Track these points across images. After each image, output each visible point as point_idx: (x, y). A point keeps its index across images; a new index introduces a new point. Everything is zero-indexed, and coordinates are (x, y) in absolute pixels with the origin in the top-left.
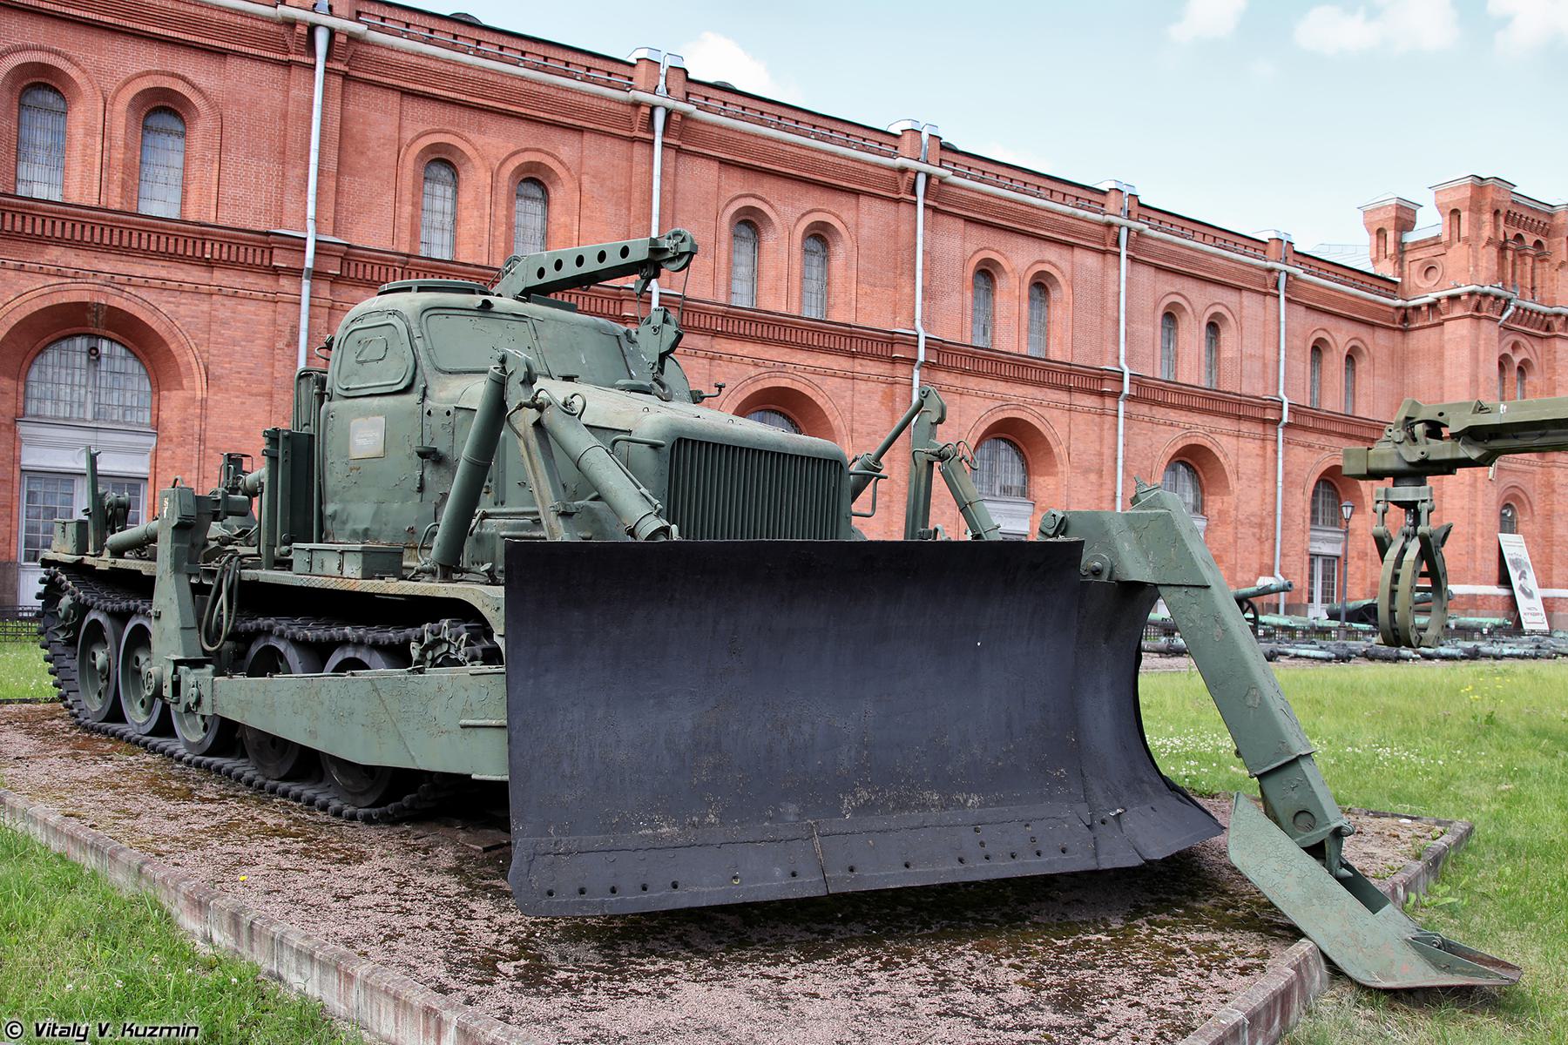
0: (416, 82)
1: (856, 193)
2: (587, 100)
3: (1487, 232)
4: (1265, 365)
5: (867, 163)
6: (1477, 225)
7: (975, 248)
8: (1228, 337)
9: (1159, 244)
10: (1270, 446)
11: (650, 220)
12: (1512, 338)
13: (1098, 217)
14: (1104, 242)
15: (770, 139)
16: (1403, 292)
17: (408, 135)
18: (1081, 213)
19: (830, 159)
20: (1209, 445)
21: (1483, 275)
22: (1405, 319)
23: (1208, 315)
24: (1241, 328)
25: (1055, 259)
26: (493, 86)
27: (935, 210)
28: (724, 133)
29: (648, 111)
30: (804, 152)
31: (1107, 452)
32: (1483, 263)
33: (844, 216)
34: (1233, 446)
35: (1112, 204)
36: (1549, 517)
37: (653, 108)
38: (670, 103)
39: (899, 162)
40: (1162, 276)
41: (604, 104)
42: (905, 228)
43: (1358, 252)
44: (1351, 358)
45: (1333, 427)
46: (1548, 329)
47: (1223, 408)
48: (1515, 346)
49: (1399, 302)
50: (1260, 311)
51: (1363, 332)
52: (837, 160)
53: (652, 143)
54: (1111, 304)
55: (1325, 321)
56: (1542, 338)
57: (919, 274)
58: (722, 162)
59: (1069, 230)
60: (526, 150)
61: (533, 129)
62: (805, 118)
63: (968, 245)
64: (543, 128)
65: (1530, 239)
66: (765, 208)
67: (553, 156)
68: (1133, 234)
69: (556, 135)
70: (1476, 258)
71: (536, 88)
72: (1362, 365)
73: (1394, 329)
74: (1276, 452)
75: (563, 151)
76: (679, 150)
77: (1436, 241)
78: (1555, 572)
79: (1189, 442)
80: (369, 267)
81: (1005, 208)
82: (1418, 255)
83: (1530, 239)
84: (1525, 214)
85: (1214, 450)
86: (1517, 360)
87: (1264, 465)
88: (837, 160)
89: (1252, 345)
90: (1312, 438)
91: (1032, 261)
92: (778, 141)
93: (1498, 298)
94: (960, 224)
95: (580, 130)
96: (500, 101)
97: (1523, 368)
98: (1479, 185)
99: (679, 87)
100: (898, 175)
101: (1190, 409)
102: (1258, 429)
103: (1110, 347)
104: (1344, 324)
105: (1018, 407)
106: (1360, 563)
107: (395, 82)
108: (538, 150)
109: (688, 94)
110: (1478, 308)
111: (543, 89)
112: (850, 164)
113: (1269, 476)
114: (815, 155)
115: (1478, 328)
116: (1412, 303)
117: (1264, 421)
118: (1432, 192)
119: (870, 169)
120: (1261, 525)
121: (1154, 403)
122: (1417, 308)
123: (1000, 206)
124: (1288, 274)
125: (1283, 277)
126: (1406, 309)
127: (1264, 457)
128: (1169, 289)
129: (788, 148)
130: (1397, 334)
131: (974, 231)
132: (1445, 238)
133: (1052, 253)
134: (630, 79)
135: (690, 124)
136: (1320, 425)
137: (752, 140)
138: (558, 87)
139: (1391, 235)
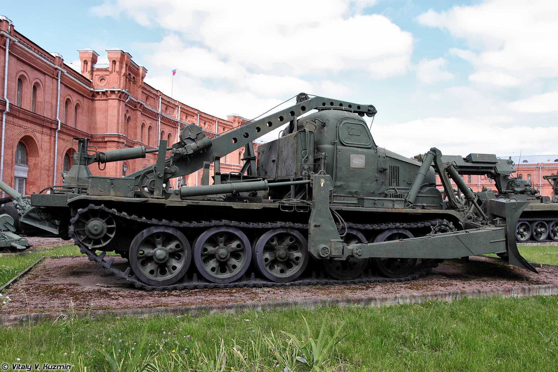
4: (52, 106)
6: (121, 68)
8: (39, 92)
20: (33, 136)
21: (122, 86)
22: (93, 96)
23: (34, 83)
24: (44, 90)
34: (42, 139)
43: (77, 66)
46: (135, 107)
47: (38, 122)
49: (92, 89)
55: (70, 92)
56: (133, 110)
65: (132, 76)
70: (120, 80)
72: (79, 111)
74: (55, 141)
77: (106, 70)
82: (99, 73)
85: (34, 138)
87: (50, 146)
89: (48, 98)
93: (126, 94)
98: (123, 54)
101: (27, 121)
102: (48, 131)
110: (120, 97)
113: (52, 150)
115: (120, 104)
116: (96, 90)
120: (49, 170)
122: (98, 93)
126: (94, 92)
127: (50, 143)
130: (90, 101)
139: (89, 64)
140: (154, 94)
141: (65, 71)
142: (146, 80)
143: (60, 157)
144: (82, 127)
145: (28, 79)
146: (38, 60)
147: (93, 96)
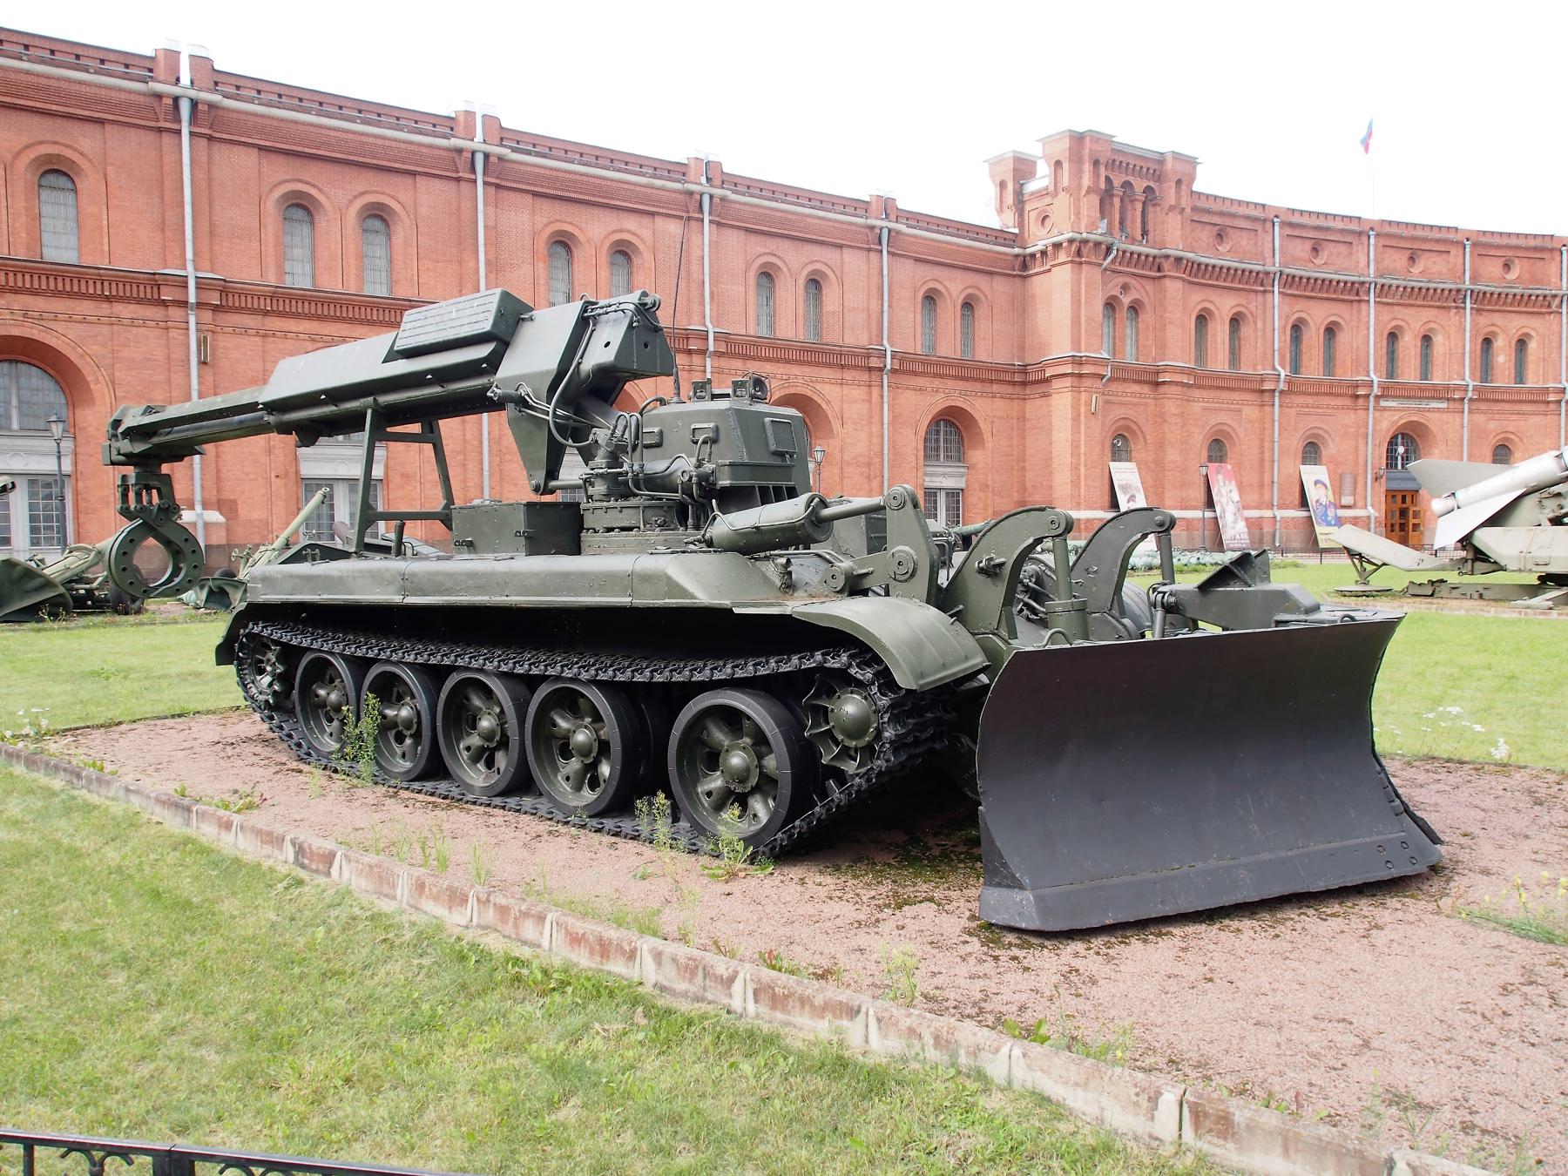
1: (414, 174)
2: (103, 92)
3: (1086, 181)
6: (1077, 174)
7: (545, 221)
8: (831, 295)
10: (875, 392)
11: (183, 207)
12: (1122, 280)
13: (678, 186)
14: (688, 209)
15: (310, 124)
16: (1024, 241)
19: (379, 142)
20: (809, 394)
21: (1084, 222)
23: (805, 272)
29: (170, 102)
30: (351, 136)
32: (1084, 210)
36: (1161, 445)
37: (176, 99)
38: (193, 93)
39: (455, 142)
40: (753, 238)
41: (123, 96)
44: (968, 306)
46: (1159, 270)
48: (1125, 288)
49: (1017, 251)
51: (982, 282)
53: (179, 132)
57: (481, 249)
58: (261, 148)
60: (42, 142)
61: (48, 122)
63: (538, 219)
64: (59, 121)
65: (1139, 185)
67: (71, 147)
71: (45, 81)
72: (981, 311)
75: (83, 143)
76: (210, 138)
78: (1167, 495)
79: (787, 392)
81: (575, 181)
83: (1139, 185)
84: (1132, 162)
85: (815, 398)
86: (1126, 300)
87: (870, 411)
88: (387, 143)
90: (922, 382)
94: (528, 199)
95: (101, 122)
97: (1135, 308)
98: (1078, 139)
100: (456, 156)
101: (788, 361)
102: (865, 377)
103: (695, 307)
104: (958, 274)
106: (982, 495)
109: (216, 84)
110: (1079, 253)
111: (52, 82)
113: (876, 419)
114: (364, 139)
115: (1079, 273)
116: (1028, 251)
117: (870, 369)
119: (424, 150)
120: (869, 465)
122: (1033, 256)
123: (569, 180)
125: (885, 232)
129: (332, 133)
131: (545, 205)
132: (1052, 188)
133: (631, 223)
134: (151, 70)
135: (220, 112)
136: (932, 369)
137: (293, 126)
140: (1248, 218)
141: (902, 228)
142: (1195, 188)
143: (909, 433)
144: (992, 347)
145: (785, 269)
147: (1025, 262)
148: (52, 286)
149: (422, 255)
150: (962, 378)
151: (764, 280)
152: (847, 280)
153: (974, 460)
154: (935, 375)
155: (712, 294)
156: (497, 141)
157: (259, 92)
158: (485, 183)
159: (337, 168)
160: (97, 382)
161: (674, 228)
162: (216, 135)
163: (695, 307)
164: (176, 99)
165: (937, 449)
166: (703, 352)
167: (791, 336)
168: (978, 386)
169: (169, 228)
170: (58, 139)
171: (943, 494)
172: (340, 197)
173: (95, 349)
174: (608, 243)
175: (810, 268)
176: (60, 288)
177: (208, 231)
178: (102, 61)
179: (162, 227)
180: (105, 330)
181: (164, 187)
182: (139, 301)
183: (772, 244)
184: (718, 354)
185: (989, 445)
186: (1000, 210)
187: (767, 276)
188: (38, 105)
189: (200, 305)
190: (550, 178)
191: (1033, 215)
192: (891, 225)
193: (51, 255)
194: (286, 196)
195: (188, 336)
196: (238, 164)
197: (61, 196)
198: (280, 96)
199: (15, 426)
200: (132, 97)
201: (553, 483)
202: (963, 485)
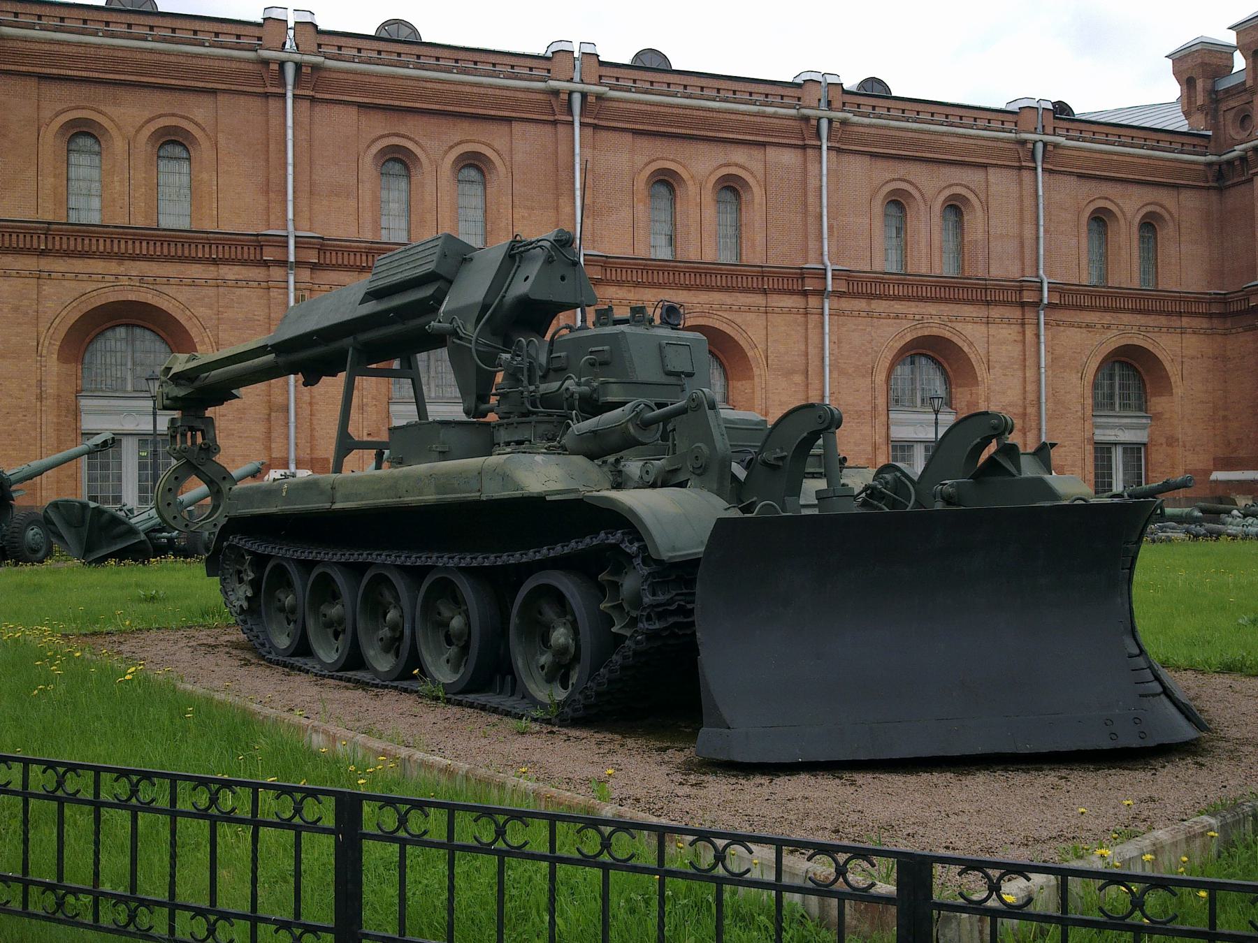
0: (51, 66)
1: (509, 120)
2: (217, 63)
5: (516, 89)
7: (646, 159)
9: (873, 131)
13: (793, 112)
17: (47, 114)
18: (770, 110)
19: (475, 90)
20: (947, 335)
23: (942, 198)
24: (986, 208)
25: (741, 160)
26: (123, 61)
27: (596, 127)
28: (358, 78)
29: (275, 67)
30: (447, 87)
31: (813, 351)
33: (496, 145)
35: (810, 96)
37: (282, 64)
38: (297, 57)
40: (881, 164)
41: (234, 65)
42: (563, 148)
45: (1120, 303)
50: (1014, 188)
52: (482, 91)
54: (811, 199)
58: (360, 105)
59: (758, 129)
60: (160, 116)
62: (446, 53)
66: (410, 145)
67: (186, 118)
68: (836, 125)
69: (191, 99)
72: (1166, 233)
73: (1209, 188)
74: (1038, 336)
75: (198, 112)
76: (313, 100)
80: (14, 236)
81: (677, 115)
82: (1232, 104)
85: (955, 339)
88: (482, 91)
91: (715, 165)
92: (418, 79)
94: (628, 137)
95: (214, 92)
96: (132, 74)
99: (310, 41)
102: (1016, 313)
104: (1136, 191)
105: (703, 314)
107: (31, 69)
108: (173, 115)
109: (319, 46)
111: (172, 59)
112: (498, 92)
114: (459, 88)
116: (1225, 157)
117: (1023, 305)
118: (1234, 33)
121: (871, 297)
122: (1230, 163)
123: (672, 115)
124: (1045, 144)
125: (1040, 146)
128: (888, 176)
129: (429, 85)
131: (644, 143)
133: (739, 155)
137: (391, 81)
138: (187, 54)
146: (945, 139)
148: (165, 252)
149: (517, 202)
150: (1140, 312)
151: (893, 210)
152: (993, 204)
153: (1159, 409)
154: (1106, 309)
155: (830, 227)
156: (595, 79)
157: (359, 50)
158: (582, 124)
159: (434, 120)
160: (203, 343)
161: (789, 158)
162: (318, 96)
163: (812, 244)
164: (282, 64)
165: (1111, 396)
166: (821, 293)
167: (924, 270)
168: (1163, 320)
169: (272, 189)
170: (175, 111)
171: (1120, 450)
172: (436, 147)
173: (201, 311)
174: (713, 179)
175: (947, 193)
176: (186, 253)
177: (308, 189)
178: (217, 35)
179: (266, 189)
180: (211, 292)
181: (268, 149)
182: (244, 263)
183: (902, 169)
184: (838, 294)
185: (1178, 390)
186: (1187, 114)
187: (898, 203)
188: (160, 81)
189: (298, 264)
190: (650, 115)
191: (1230, 115)
192: (1046, 138)
193: (167, 222)
194: (382, 151)
195: (287, 295)
196: (339, 123)
197: (174, 166)
198: (379, 52)
199: (129, 388)
200: (242, 66)
201: (484, 407)
202: (1145, 440)
